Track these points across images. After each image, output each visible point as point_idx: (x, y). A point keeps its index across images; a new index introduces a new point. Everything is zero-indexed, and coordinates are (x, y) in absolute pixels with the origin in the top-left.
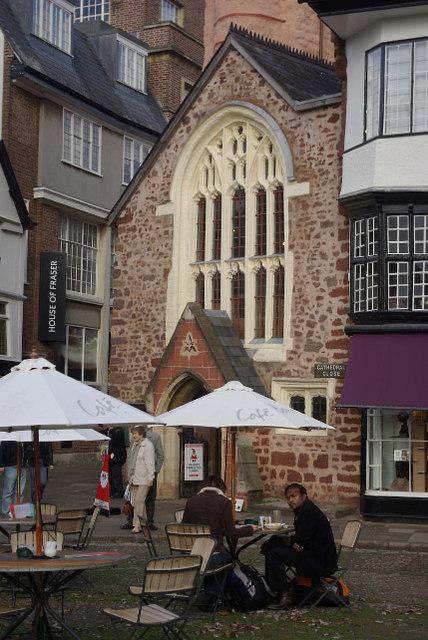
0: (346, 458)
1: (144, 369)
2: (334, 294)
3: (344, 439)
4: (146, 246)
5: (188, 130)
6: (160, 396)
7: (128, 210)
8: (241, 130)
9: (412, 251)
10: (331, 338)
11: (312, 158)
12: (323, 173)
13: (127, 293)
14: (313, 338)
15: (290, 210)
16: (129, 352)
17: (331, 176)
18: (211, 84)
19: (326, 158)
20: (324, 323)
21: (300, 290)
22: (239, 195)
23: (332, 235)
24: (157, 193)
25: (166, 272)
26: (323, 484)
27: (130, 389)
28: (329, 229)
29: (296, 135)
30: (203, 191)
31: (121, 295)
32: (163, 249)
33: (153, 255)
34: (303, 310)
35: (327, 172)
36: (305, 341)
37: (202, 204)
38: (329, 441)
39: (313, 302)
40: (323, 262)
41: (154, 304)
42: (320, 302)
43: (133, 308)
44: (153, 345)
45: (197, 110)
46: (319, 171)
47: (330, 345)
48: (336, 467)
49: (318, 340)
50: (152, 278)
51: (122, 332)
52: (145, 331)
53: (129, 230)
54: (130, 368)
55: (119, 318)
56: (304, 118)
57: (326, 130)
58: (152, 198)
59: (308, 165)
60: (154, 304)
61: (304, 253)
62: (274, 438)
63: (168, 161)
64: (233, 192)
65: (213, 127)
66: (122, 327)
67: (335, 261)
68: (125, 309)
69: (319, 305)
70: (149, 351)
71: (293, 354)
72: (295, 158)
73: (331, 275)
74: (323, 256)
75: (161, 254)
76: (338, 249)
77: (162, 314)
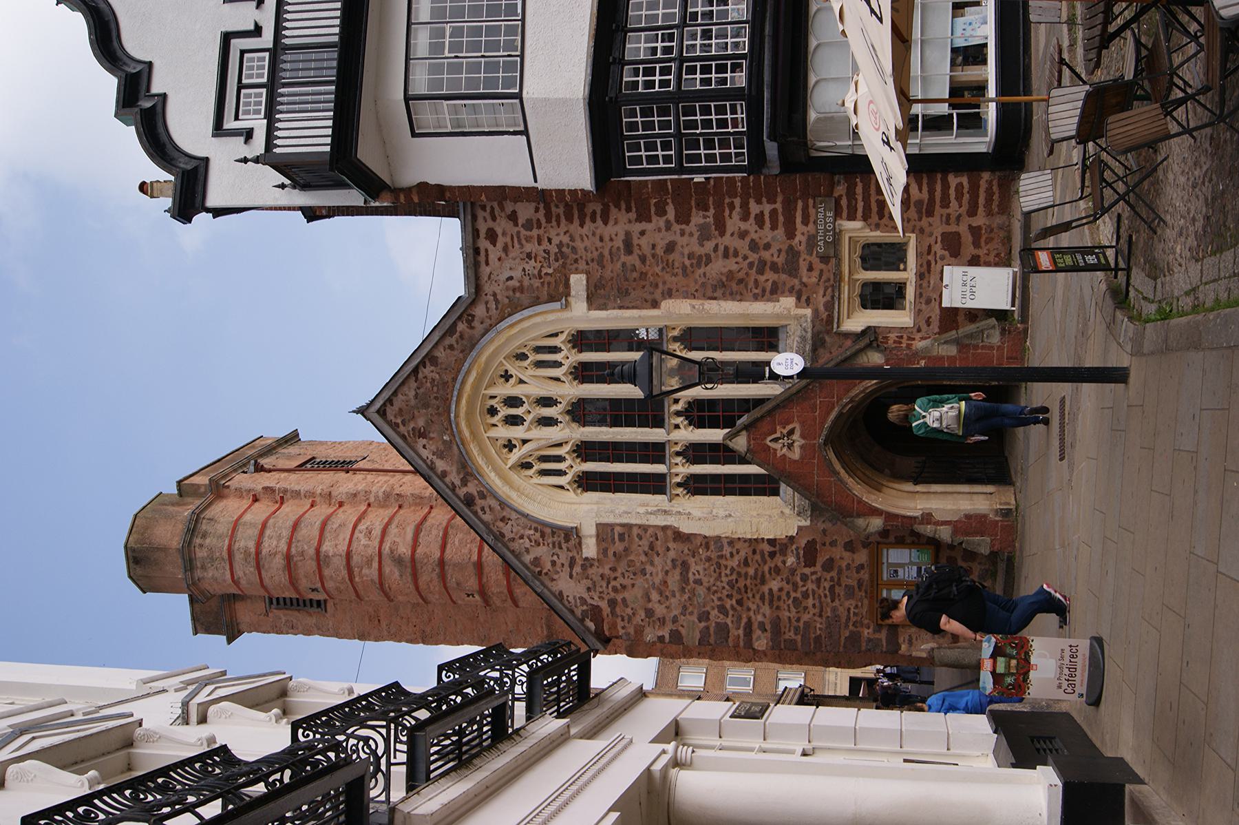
0: (945, 203)
1: (818, 581)
2: (721, 227)
3: (919, 203)
4: (640, 581)
5: (483, 496)
6: (860, 501)
7: (584, 613)
8: (493, 411)
9: (670, 60)
10: (780, 232)
11: (540, 271)
12: (560, 255)
13: (704, 616)
14: (780, 260)
15: (603, 307)
16: (793, 614)
17: (566, 239)
18: (425, 453)
19: (542, 248)
20: (761, 243)
21: (715, 288)
22: (581, 412)
23: (643, 233)
24: (564, 558)
25: (679, 536)
26: (983, 244)
27: (849, 610)
28: (635, 242)
29: (506, 301)
30: (569, 477)
31: (707, 628)
32: (645, 543)
33: (652, 564)
34: (741, 281)
35: (560, 245)
36: (784, 277)
37: (587, 482)
38: (922, 231)
39: (731, 264)
40: (678, 248)
41: (723, 562)
42: (731, 251)
43: (729, 603)
44: (784, 562)
45: (457, 482)
46: (557, 260)
47: (791, 234)
48: (959, 218)
49: (783, 255)
50: (685, 566)
51: (762, 626)
52: (763, 582)
53: (613, 613)
54: (817, 611)
55: (741, 632)
56: (488, 288)
57: (505, 249)
58: (572, 565)
59: (548, 279)
60: (723, 562)
61: (664, 283)
62: (919, 330)
63: (522, 537)
64: (574, 425)
65: (483, 451)
66: (755, 626)
67: (676, 227)
68: (729, 621)
69: (736, 254)
70: (793, 571)
71: (802, 297)
72: (536, 302)
73: (697, 235)
74: (670, 248)
75: (652, 547)
76: (662, 223)
77: (739, 545)
